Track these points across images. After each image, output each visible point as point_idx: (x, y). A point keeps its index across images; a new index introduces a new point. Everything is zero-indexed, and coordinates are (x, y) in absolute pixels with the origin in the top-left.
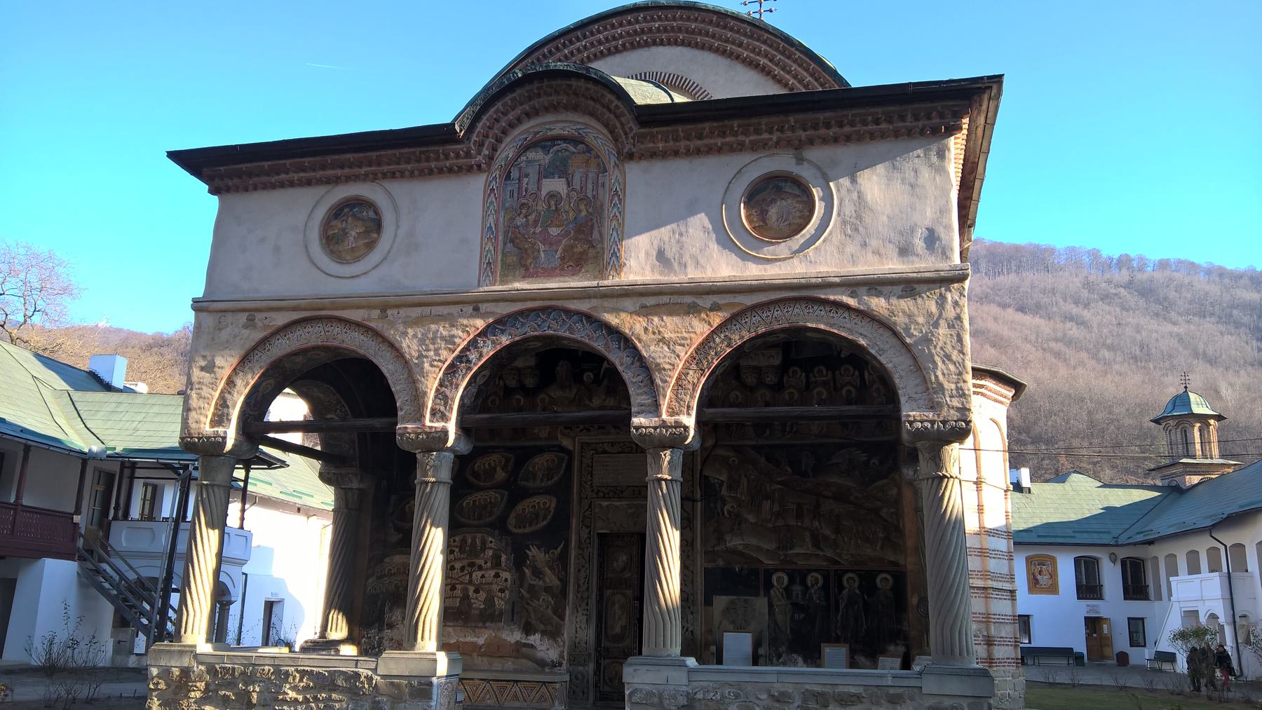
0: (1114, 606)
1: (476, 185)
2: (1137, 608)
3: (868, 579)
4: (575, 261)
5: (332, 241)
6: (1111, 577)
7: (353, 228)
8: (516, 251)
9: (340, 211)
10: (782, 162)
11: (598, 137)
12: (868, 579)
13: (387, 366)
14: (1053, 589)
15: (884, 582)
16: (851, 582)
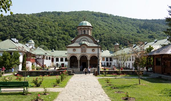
0: (109, 62)
1: (80, 48)
2: (111, 62)
3: (95, 64)
4: (85, 52)
5: (73, 51)
6: (109, 59)
7: (74, 50)
8: (82, 51)
9: (74, 49)
10: (93, 48)
11: (86, 47)
12: (95, 64)
13: (77, 57)
14: (104, 60)
15: (96, 64)
16: (94, 64)
